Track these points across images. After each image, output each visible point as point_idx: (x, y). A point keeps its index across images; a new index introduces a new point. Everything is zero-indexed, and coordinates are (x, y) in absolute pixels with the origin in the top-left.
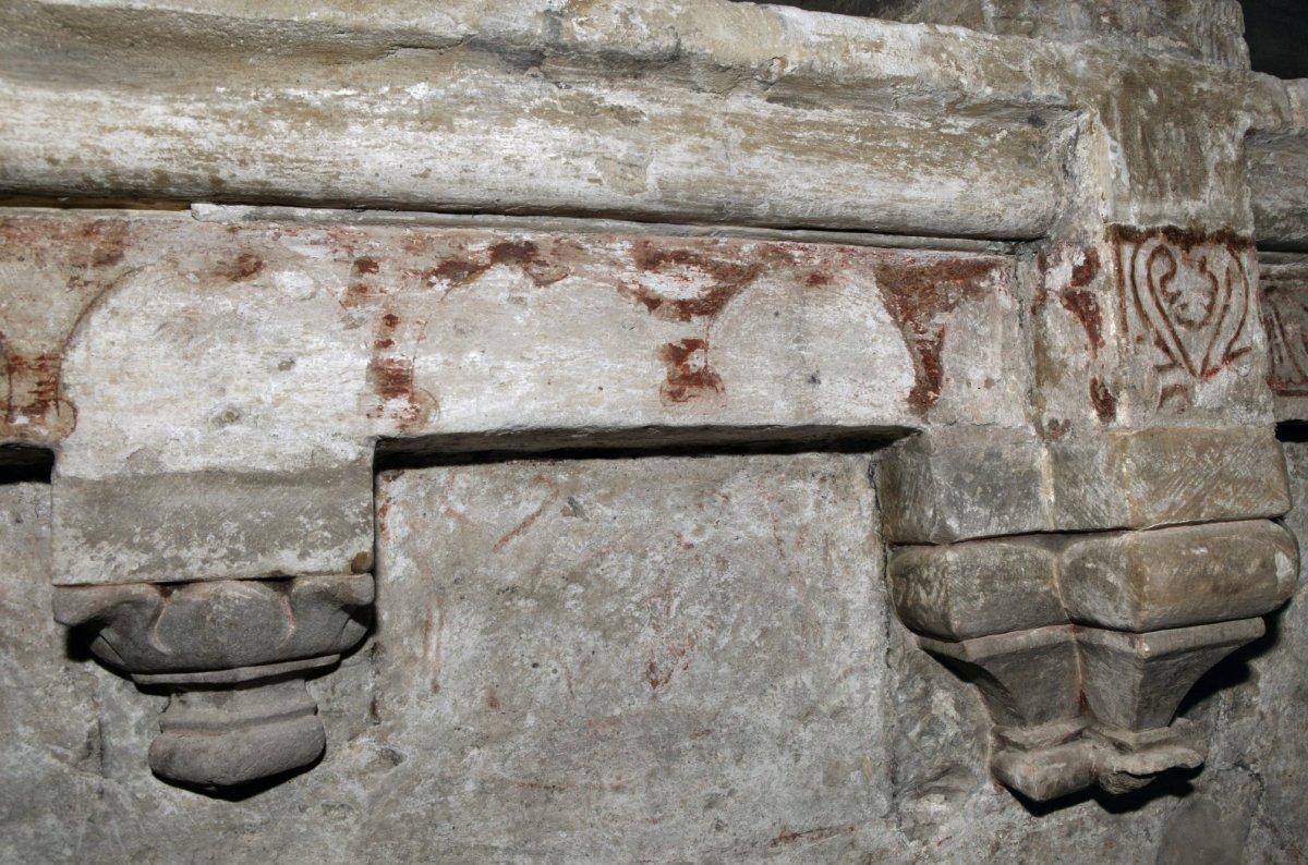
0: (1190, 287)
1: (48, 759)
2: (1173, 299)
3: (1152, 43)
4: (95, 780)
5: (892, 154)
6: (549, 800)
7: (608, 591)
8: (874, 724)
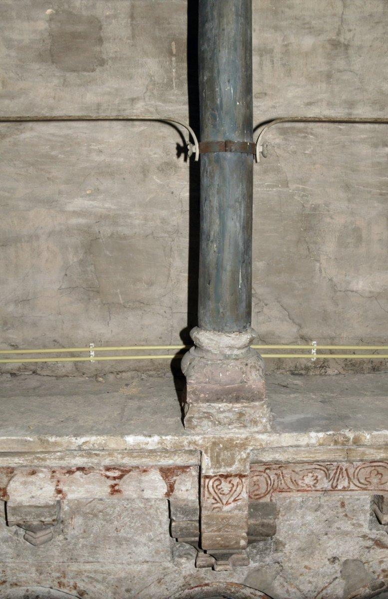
0: (225, 486)
1: (9, 534)
2: (219, 489)
3: (230, 427)
4: (17, 538)
5: (156, 456)
6: (95, 549)
7: (107, 514)
8: (168, 543)
